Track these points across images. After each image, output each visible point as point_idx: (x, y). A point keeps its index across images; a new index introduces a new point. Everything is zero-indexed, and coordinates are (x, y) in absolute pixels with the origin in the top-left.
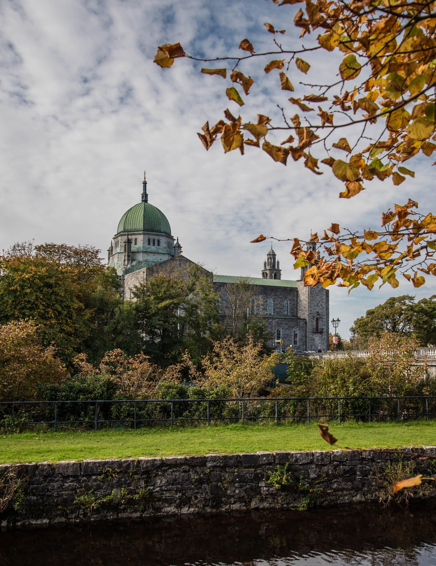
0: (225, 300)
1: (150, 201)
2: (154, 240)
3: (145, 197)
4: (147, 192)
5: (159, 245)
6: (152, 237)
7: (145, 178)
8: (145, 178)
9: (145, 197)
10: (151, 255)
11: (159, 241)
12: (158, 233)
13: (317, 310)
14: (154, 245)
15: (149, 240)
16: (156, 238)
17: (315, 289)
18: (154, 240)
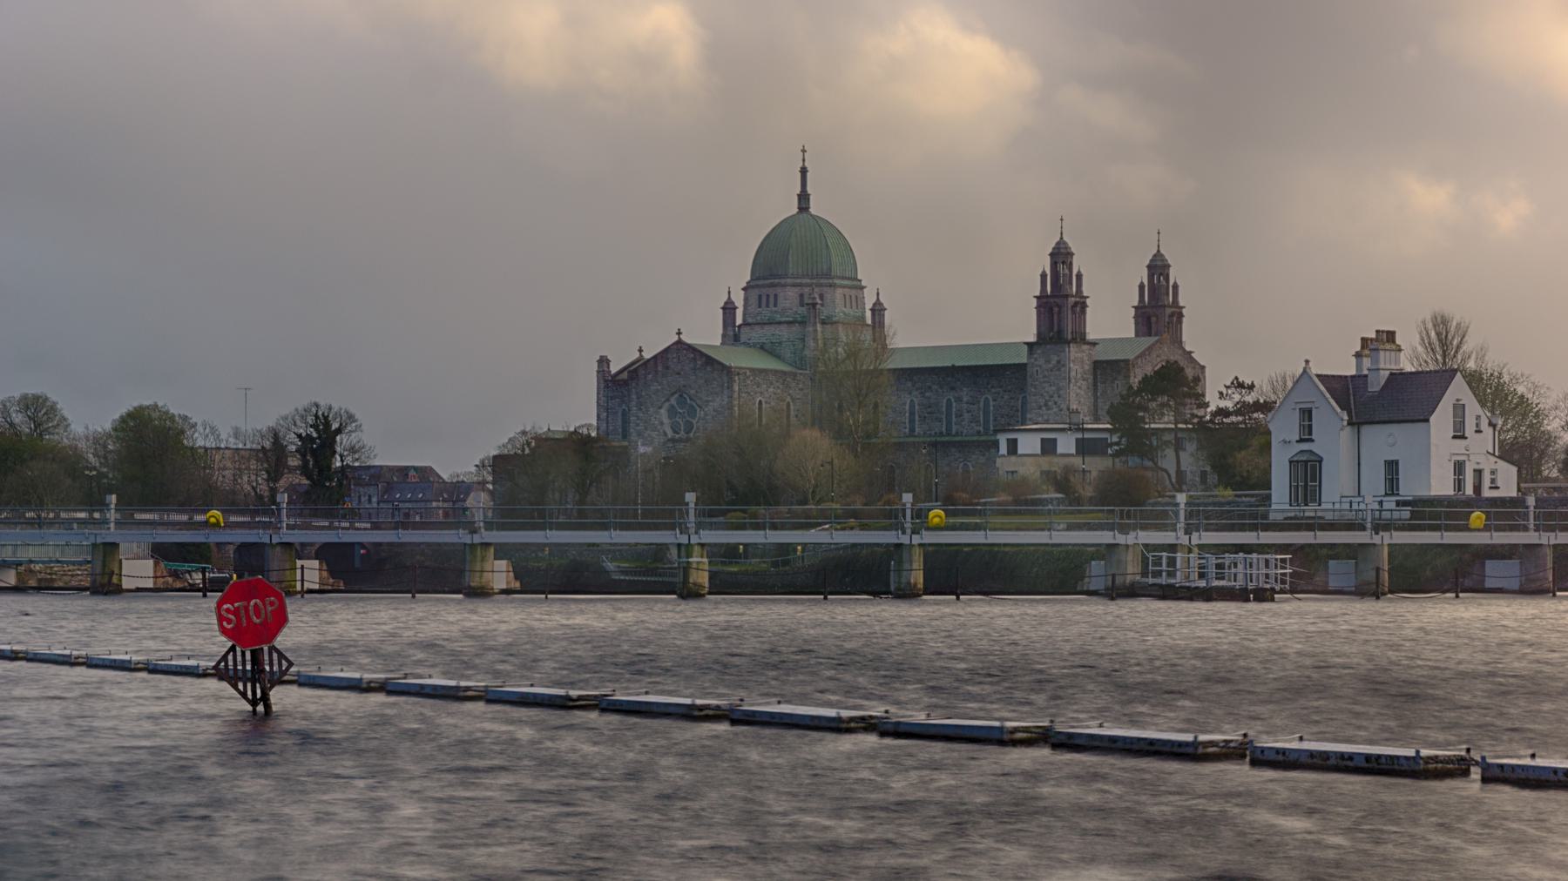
1: (814, 209)
2: (768, 296)
3: (804, 198)
4: (809, 190)
5: (775, 305)
6: (764, 291)
7: (804, 160)
8: (804, 160)
9: (804, 198)
10: (757, 328)
11: (776, 296)
12: (776, 281)
13: (1046, 417)
14: (767, 306)
15: (760, 297)
16: (771, 291)
17: (1040, 366)
18: (768, 296)
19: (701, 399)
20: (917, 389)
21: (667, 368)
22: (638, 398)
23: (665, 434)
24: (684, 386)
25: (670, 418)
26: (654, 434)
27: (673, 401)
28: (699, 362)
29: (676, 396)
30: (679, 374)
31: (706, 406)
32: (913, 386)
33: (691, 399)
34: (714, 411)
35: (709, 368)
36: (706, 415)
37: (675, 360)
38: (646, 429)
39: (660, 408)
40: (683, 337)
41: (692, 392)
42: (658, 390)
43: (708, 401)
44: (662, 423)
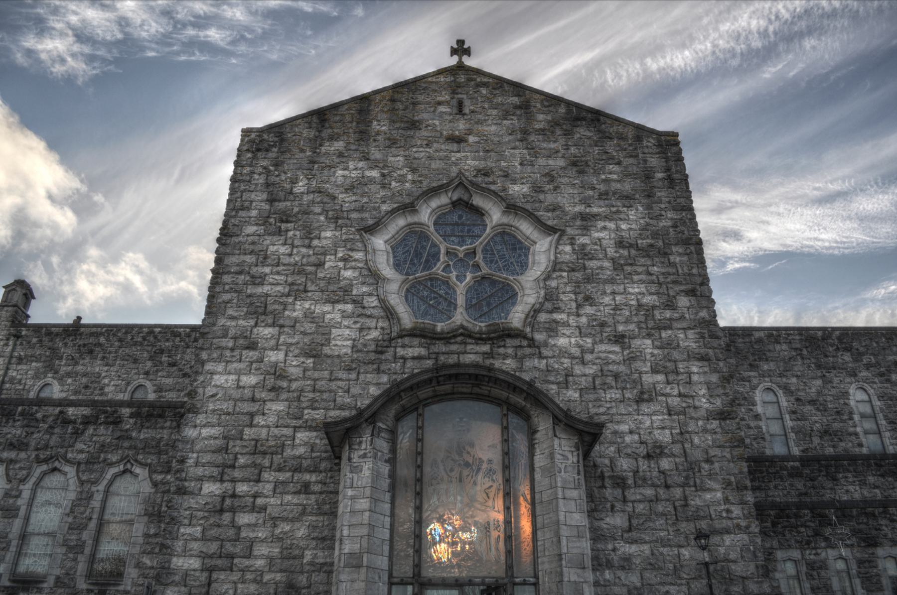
0: (812, 402)
19: (555, 208)
20: (868, 366)
21: (414, 125)
22: (271, 201)
23: (389, 313)
24: (486, 173)
25: (397, 266)
26: (332, 313)
27: (425, 215)
28: (541, 117)
29: (443, 200)
30: (459, 140)
31: (585, 230)
32: (856, 360)
33: (511, 208)
34: (620, 244)
35: (582, 132)
36: (583, 254)
37: (442, 109)
38: (299, 292)
39: (371, 229)
40: (469, 62)
41: (518, 190)
42: (363, 182)
43: (584, 217)
44: (374, 277)
